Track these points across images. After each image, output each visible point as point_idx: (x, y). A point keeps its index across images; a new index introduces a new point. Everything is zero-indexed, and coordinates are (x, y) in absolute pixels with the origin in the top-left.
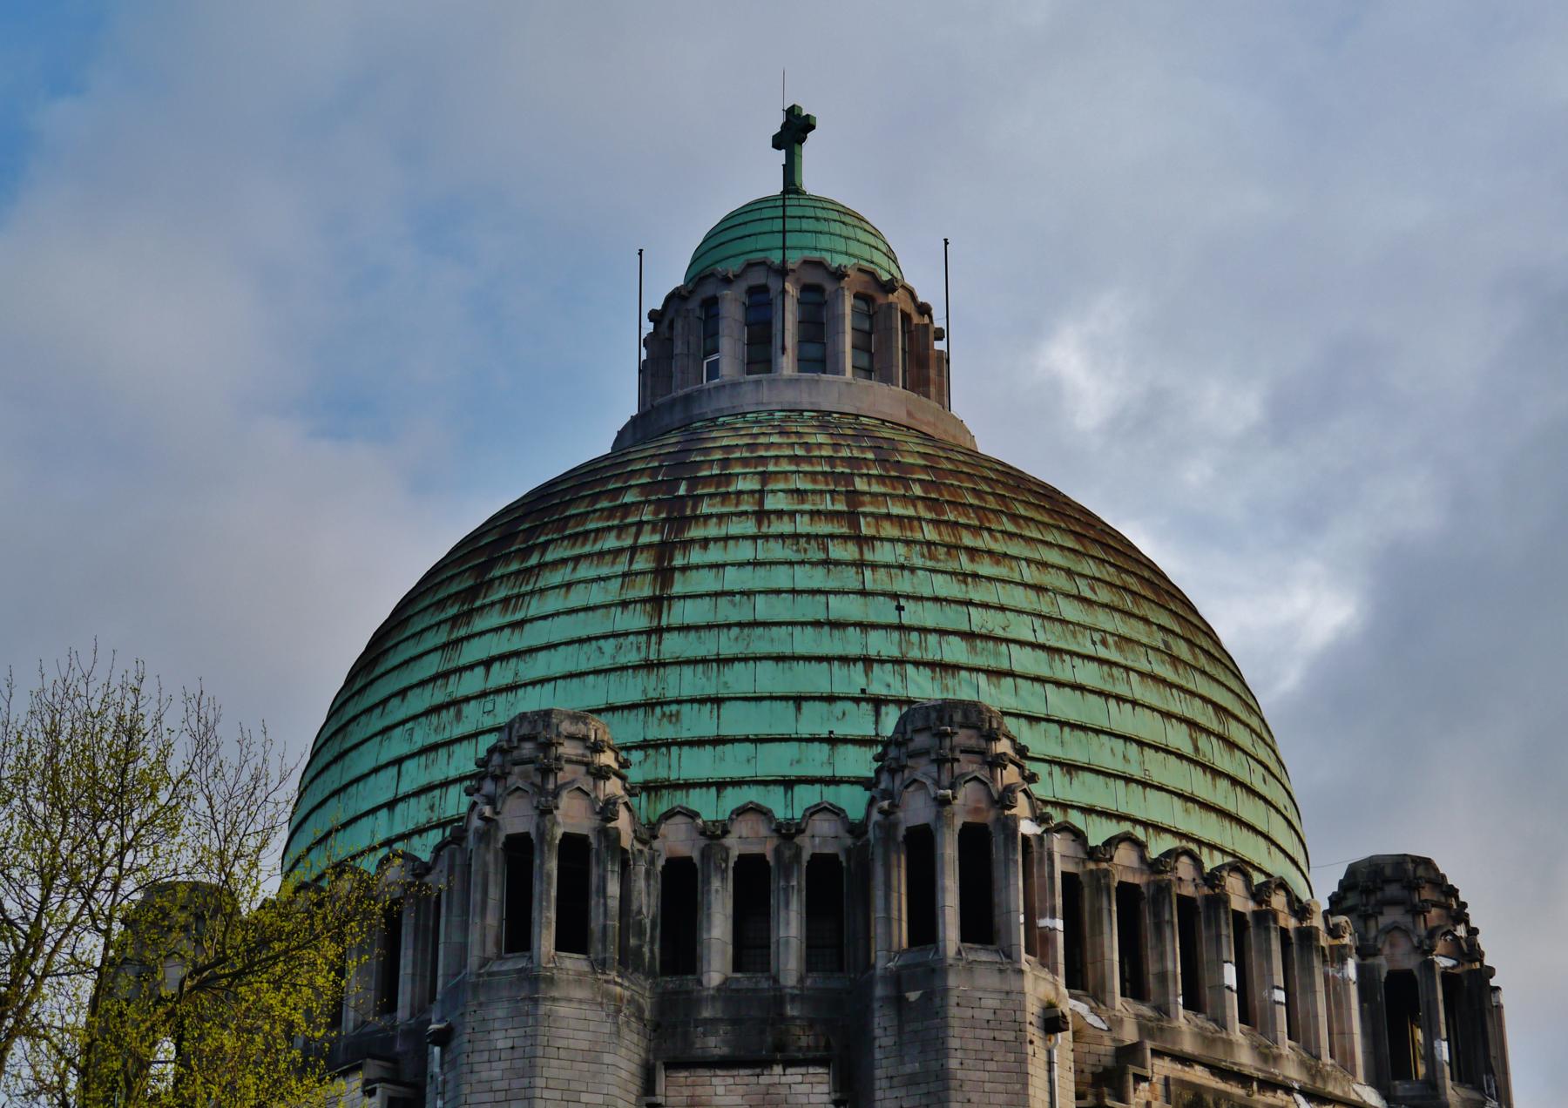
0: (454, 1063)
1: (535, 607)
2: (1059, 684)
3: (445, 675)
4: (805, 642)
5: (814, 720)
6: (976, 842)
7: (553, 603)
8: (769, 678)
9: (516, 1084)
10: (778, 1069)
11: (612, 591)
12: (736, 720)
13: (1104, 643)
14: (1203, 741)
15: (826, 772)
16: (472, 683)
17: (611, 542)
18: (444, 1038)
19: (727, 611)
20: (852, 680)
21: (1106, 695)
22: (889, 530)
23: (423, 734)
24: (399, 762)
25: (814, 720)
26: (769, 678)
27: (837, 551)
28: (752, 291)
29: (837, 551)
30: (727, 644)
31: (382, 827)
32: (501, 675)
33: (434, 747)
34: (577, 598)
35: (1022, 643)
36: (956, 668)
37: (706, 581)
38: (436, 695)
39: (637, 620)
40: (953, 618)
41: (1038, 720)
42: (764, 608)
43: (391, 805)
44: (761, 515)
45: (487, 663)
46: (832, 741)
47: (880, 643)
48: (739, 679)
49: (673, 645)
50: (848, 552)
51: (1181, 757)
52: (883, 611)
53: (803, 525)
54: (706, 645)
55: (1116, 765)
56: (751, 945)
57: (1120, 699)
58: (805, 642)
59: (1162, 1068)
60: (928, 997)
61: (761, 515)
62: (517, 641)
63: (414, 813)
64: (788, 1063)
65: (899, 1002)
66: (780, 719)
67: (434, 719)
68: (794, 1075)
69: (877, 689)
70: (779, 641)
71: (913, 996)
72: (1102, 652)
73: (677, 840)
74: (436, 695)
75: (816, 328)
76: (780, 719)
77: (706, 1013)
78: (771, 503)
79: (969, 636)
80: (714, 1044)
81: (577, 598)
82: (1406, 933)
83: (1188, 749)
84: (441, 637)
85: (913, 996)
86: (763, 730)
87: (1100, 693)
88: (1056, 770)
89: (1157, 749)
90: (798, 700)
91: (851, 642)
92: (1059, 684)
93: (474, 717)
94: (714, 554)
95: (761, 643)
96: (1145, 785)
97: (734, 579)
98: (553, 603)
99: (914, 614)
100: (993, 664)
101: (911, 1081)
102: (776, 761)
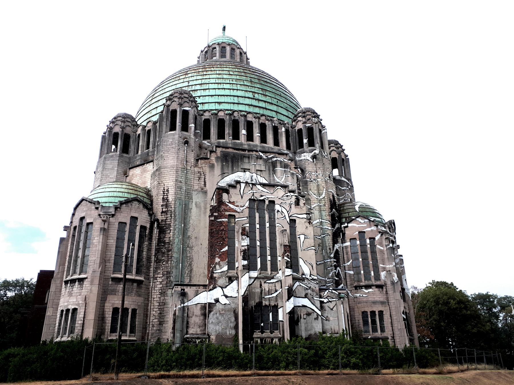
2: (219, 89)
13: (232, 81)
14: (256, 95)
21: (231, 89)
35: (212, 83)
36: (197, 90)
41: (213, 96)
51: (249, 98)
55: (230, 101)
57: (233, 89)
59: (219, 150)
72: (231, 82)
83: (252, 97)
87: (229, 89)
88: (217, 104)
89: (242, 97)
92: (219, 89)
96: (238, 104)
100: (205, 88)
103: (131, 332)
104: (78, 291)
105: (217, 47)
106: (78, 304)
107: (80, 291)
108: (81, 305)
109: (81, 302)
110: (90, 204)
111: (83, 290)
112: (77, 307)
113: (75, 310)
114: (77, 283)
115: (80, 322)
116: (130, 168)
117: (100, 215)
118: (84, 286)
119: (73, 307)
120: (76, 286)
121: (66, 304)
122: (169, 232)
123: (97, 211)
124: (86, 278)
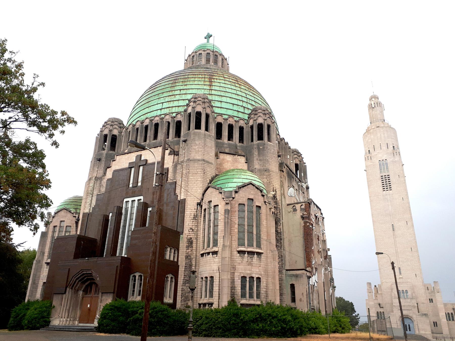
0: (187, 145)
1: (188, 83)
3: (172, 91)
4: (234, 96)
5: (235, 108)
6: (269, 126)
7: (191, 83)
8: (229, 100)
9: (200, 150)
10: (237, 156)
11: (202, 83)
12: (224, 105)
15: (237, 116)
16: (178, 92)
17: (200, 76)
18: (185, 141)
19: (221, 89)
20: (240, 103)
22: (242, 84)
23: (167, 99)
24: (163, 103)
25: (235, 108)
26: (229, 100)
27: (236, 85)
28: (207, 53)
29: (236, 85)
30: (222, 94)
31: (159, 113)
32: (182, 92)
33: (170, 101)
34: (196, 83)
37: (218, 85)
38: (171, 94)
39: (208, 87)
40: (253, 99)
42: (227, 90)
43: (161, 109)
44: (224, 77)
45: (180, 90)
46: (238, 111)
47: (244, 99)
48: (224, 99)
49: (213, 92)
50: (238, 86)
52: (244, 95)
53: (231, 80)
54: (219, 93)
56: (230, 137)
58: (234, 96)
60: (264, 148)
61: (224, 77)
62: (185, 87)
63: (167, 111)
64: (238, 155)
65: (259, 148)
66: (230, 106)
67: (170, 97)
68: (239, 157)
69: (244, 105)
70: (230, 95)
71: (261, 147)
73: (219, 119)
74: (171, 94)
75: (216, 62)
76: (230, 106)
77: (225, 146)
78: (225, 76)
79: (255, 101)
80: (227, 151)
81: (196, 83)
82: (298, 158)
84: (170, 85)
85: (261, 147)
86: (228, 108)
90: (233, 104)
91: (240, 98)
93: (190, 91)
94: (218, 81)
95: (227, 95)
97: (222, 85)
98: (191, 83)
99: (248, 96)
101: (260, 160)
102: (230, 113)
103: (249, 298)
104: (258, 263)
105: (211, 53)
106: (261, 275)
107: (260, 263)
108: (263, 275)
109: (263, 273)
110: (257, 189)
111: (262, 263)
112: (260, 277)
113: (259, 279)
114: (255, 256)
115: (264, 290)
116: (220, 152)
117: (265, 202)
118: (262, 259)
119: (257, 276)
120: (256, 258)
121: (249, 272)
122: (279, 224)
123: (262, 198)
124: (262, 253)
